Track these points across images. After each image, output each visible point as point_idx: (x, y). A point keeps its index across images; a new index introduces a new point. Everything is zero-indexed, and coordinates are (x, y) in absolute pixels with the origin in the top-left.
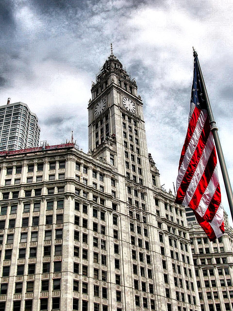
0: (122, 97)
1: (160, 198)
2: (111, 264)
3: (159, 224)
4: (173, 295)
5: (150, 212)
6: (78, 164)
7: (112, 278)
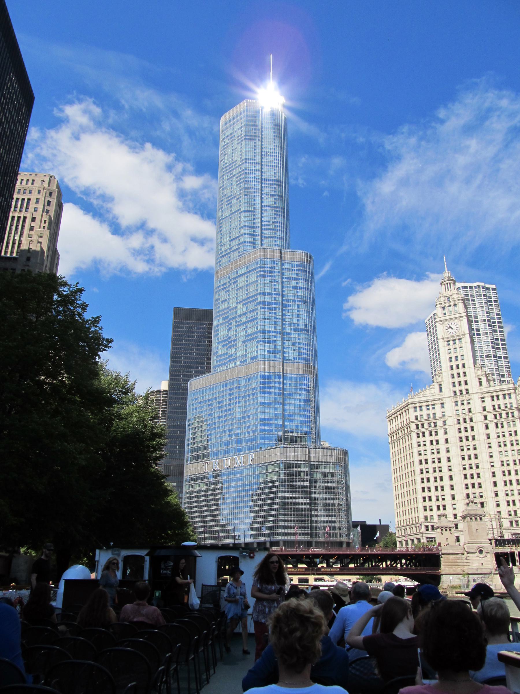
0: (444, 326)
1: (485, 395)
2: (444, 460)
3: (485, 418)
6: (415, 408)
7: (445, 469)
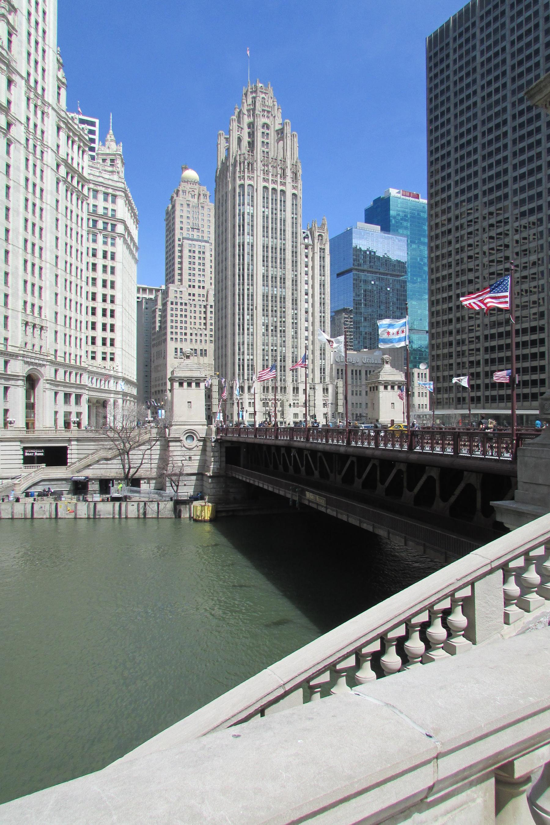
1: (62, 125)
3: (58, 166)
4: (61, 264)
5: (50, 145)
